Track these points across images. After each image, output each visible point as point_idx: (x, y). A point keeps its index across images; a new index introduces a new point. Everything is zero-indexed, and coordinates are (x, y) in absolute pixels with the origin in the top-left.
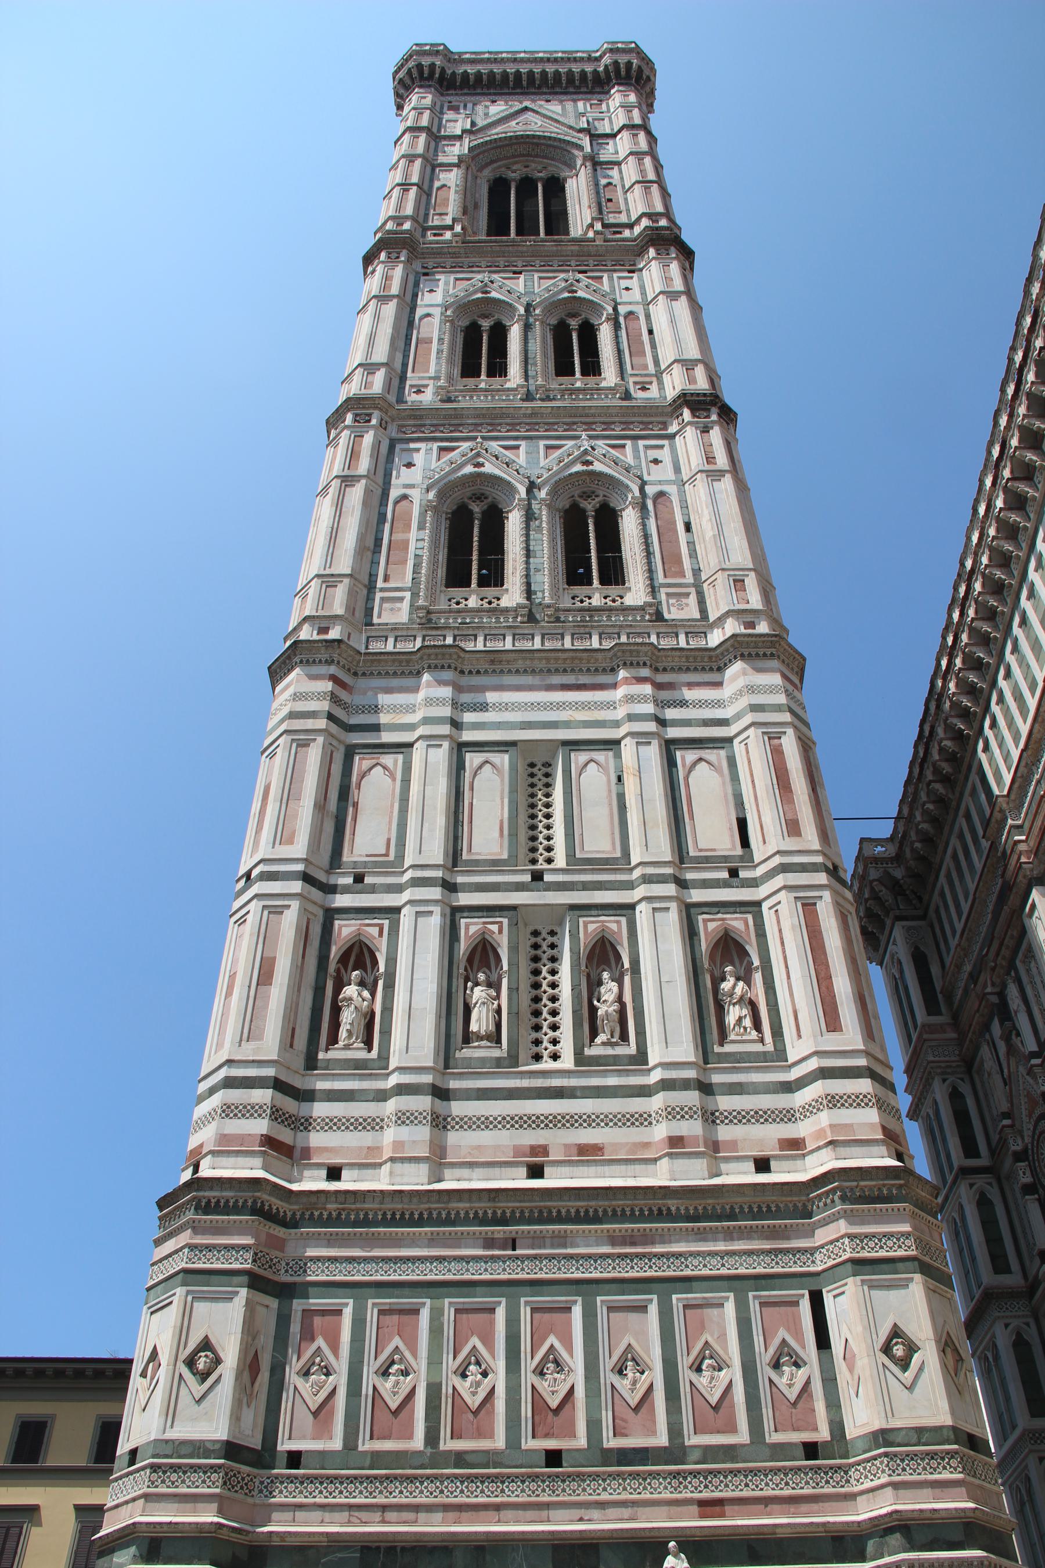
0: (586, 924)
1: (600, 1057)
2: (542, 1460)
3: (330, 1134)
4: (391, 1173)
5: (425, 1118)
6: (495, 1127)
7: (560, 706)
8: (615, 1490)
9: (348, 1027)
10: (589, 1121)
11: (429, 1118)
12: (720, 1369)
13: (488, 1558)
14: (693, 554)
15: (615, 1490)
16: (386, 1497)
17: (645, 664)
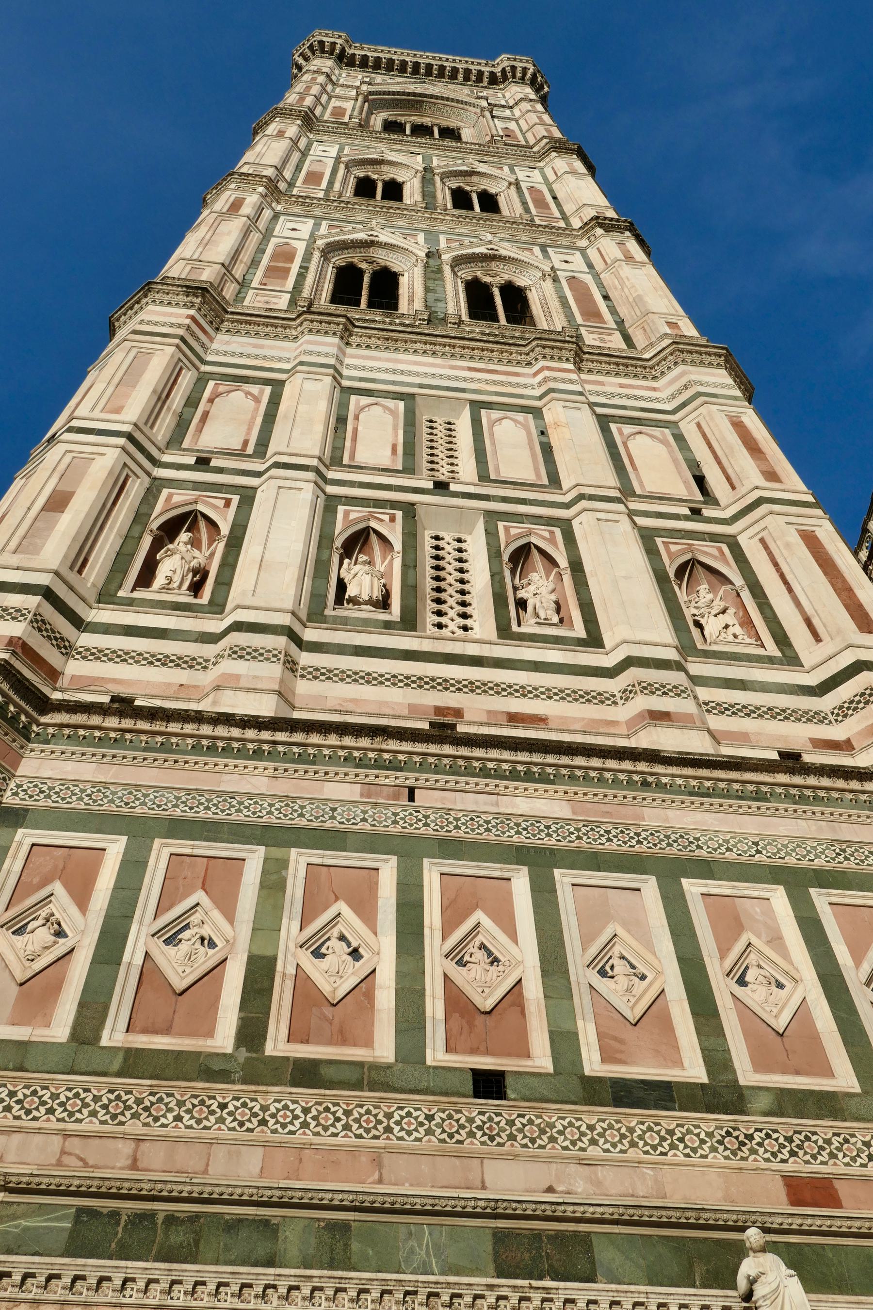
0: (507, 529)
1: (535, 634)
2: (468, 1085)
3: (122, 666)
4: (215, 703)
5: (275, 656)
6: (381, 683)
7: (465, 379)
8: (614, 1145)
9: (170, 574)
10: (524, 692)
11: (282, 656)
12: (780, 986)
13: (355, 1246)
14: (613, 311)
15: (614, 1145)
16: (146, 1125)
17: (567, 360)
